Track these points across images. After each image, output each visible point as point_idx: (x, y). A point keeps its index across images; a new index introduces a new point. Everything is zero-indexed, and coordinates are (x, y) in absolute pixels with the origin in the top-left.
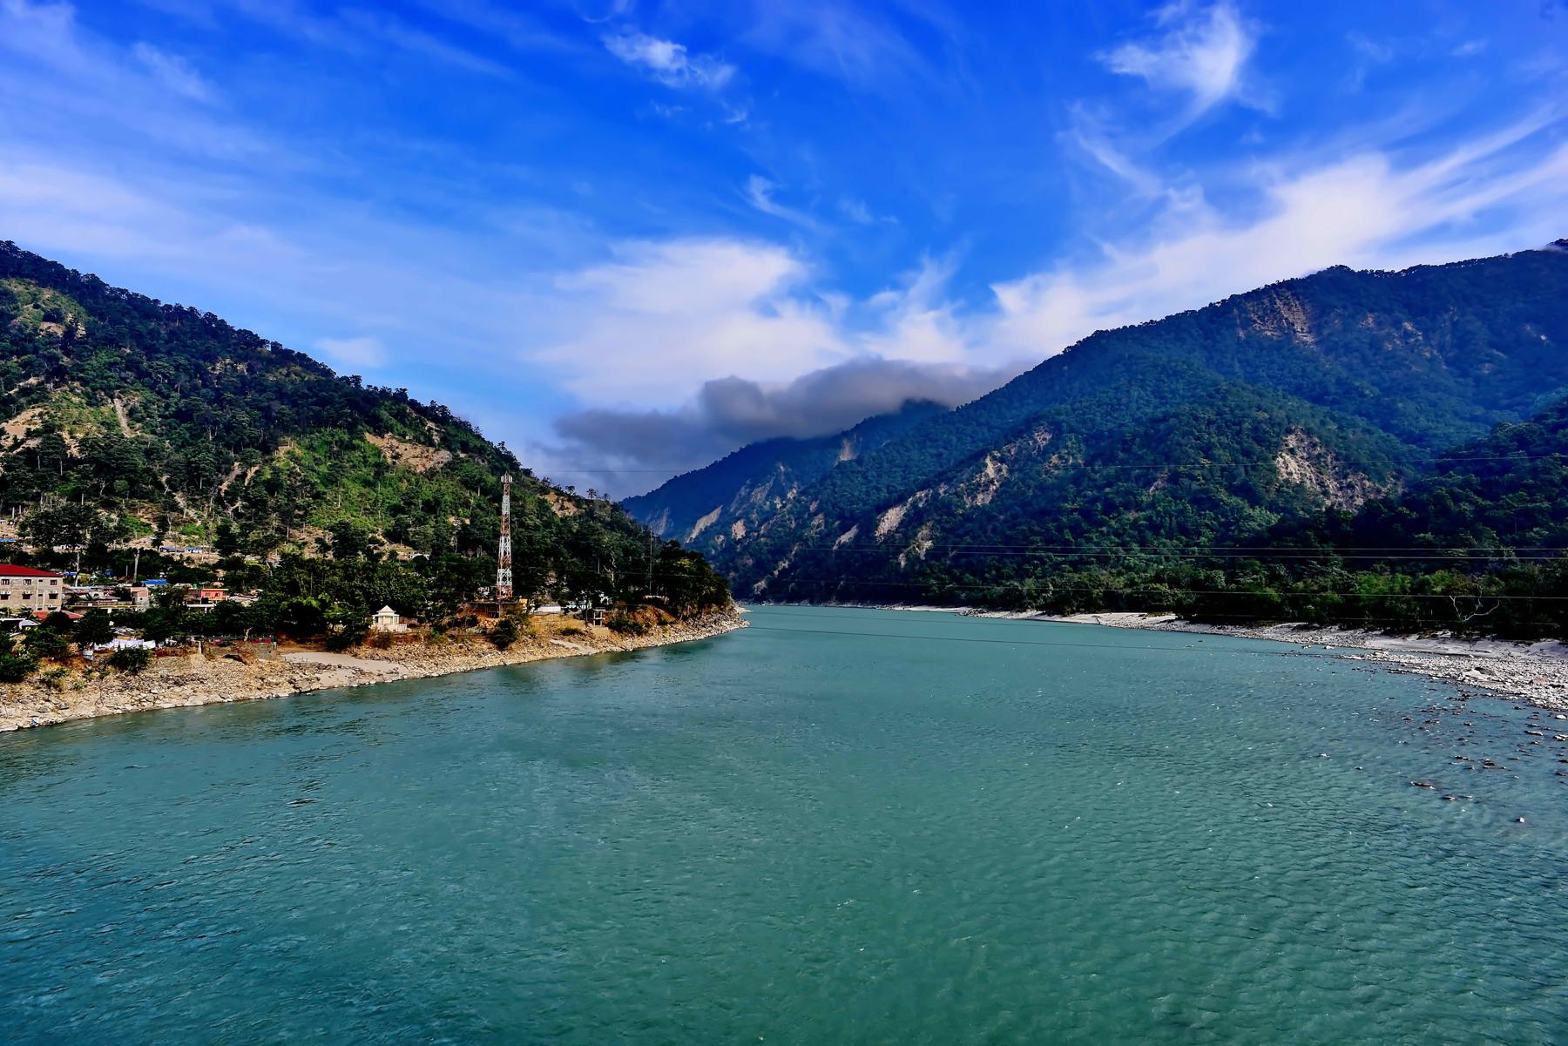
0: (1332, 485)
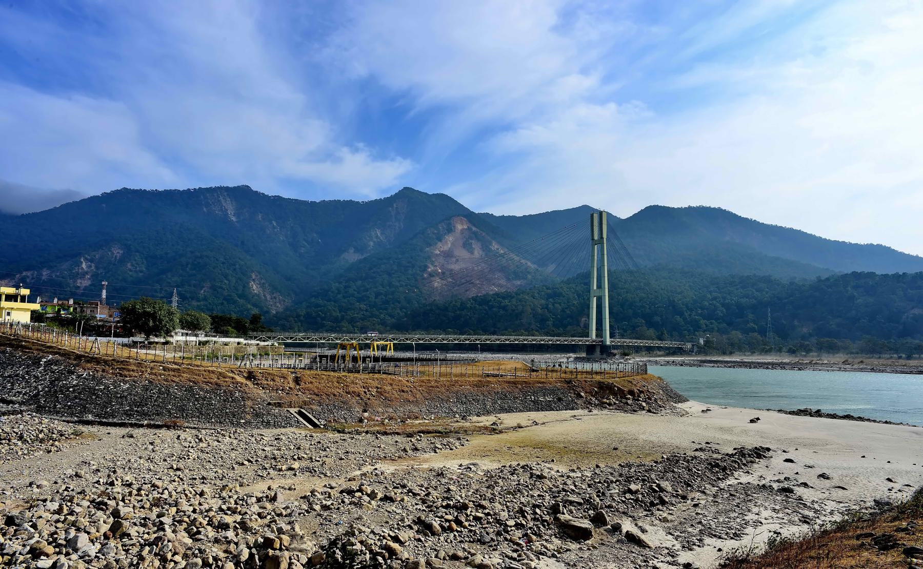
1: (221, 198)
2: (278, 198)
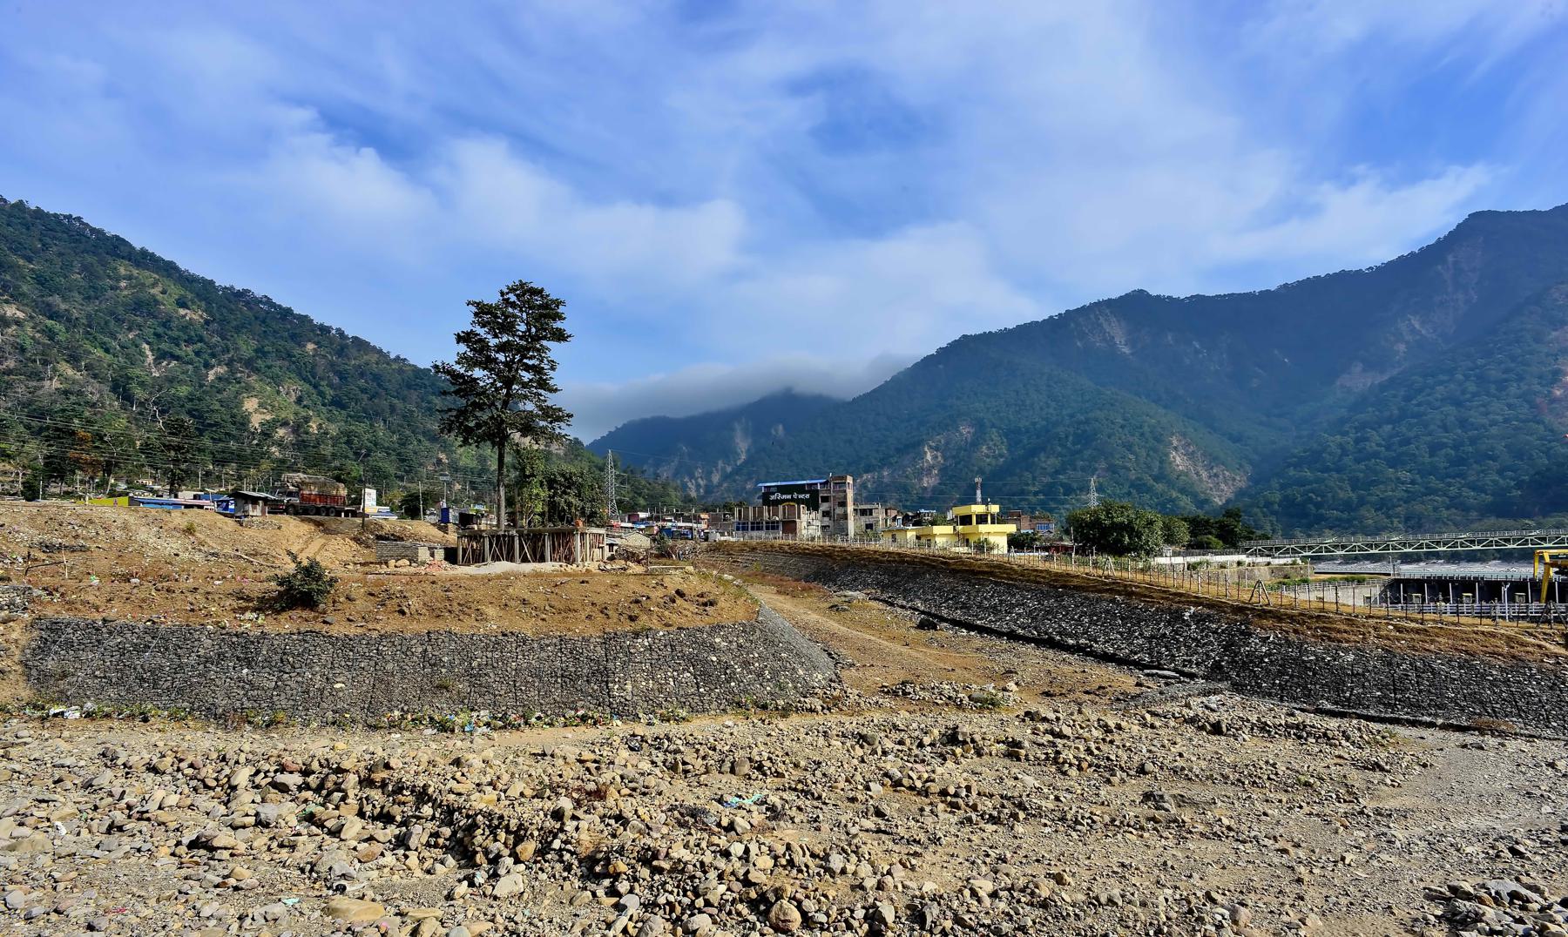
0: (1204, 474)
1: (1102, 320)
2: (1198, 300)
